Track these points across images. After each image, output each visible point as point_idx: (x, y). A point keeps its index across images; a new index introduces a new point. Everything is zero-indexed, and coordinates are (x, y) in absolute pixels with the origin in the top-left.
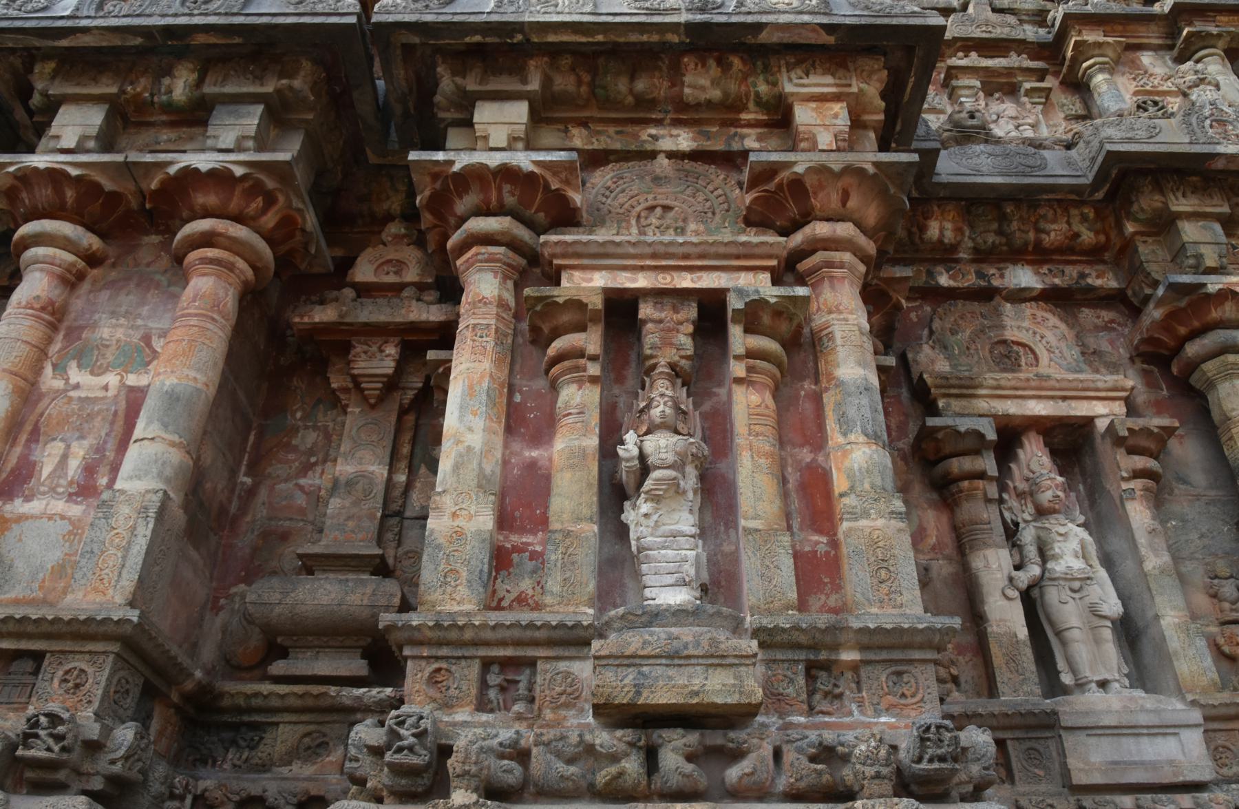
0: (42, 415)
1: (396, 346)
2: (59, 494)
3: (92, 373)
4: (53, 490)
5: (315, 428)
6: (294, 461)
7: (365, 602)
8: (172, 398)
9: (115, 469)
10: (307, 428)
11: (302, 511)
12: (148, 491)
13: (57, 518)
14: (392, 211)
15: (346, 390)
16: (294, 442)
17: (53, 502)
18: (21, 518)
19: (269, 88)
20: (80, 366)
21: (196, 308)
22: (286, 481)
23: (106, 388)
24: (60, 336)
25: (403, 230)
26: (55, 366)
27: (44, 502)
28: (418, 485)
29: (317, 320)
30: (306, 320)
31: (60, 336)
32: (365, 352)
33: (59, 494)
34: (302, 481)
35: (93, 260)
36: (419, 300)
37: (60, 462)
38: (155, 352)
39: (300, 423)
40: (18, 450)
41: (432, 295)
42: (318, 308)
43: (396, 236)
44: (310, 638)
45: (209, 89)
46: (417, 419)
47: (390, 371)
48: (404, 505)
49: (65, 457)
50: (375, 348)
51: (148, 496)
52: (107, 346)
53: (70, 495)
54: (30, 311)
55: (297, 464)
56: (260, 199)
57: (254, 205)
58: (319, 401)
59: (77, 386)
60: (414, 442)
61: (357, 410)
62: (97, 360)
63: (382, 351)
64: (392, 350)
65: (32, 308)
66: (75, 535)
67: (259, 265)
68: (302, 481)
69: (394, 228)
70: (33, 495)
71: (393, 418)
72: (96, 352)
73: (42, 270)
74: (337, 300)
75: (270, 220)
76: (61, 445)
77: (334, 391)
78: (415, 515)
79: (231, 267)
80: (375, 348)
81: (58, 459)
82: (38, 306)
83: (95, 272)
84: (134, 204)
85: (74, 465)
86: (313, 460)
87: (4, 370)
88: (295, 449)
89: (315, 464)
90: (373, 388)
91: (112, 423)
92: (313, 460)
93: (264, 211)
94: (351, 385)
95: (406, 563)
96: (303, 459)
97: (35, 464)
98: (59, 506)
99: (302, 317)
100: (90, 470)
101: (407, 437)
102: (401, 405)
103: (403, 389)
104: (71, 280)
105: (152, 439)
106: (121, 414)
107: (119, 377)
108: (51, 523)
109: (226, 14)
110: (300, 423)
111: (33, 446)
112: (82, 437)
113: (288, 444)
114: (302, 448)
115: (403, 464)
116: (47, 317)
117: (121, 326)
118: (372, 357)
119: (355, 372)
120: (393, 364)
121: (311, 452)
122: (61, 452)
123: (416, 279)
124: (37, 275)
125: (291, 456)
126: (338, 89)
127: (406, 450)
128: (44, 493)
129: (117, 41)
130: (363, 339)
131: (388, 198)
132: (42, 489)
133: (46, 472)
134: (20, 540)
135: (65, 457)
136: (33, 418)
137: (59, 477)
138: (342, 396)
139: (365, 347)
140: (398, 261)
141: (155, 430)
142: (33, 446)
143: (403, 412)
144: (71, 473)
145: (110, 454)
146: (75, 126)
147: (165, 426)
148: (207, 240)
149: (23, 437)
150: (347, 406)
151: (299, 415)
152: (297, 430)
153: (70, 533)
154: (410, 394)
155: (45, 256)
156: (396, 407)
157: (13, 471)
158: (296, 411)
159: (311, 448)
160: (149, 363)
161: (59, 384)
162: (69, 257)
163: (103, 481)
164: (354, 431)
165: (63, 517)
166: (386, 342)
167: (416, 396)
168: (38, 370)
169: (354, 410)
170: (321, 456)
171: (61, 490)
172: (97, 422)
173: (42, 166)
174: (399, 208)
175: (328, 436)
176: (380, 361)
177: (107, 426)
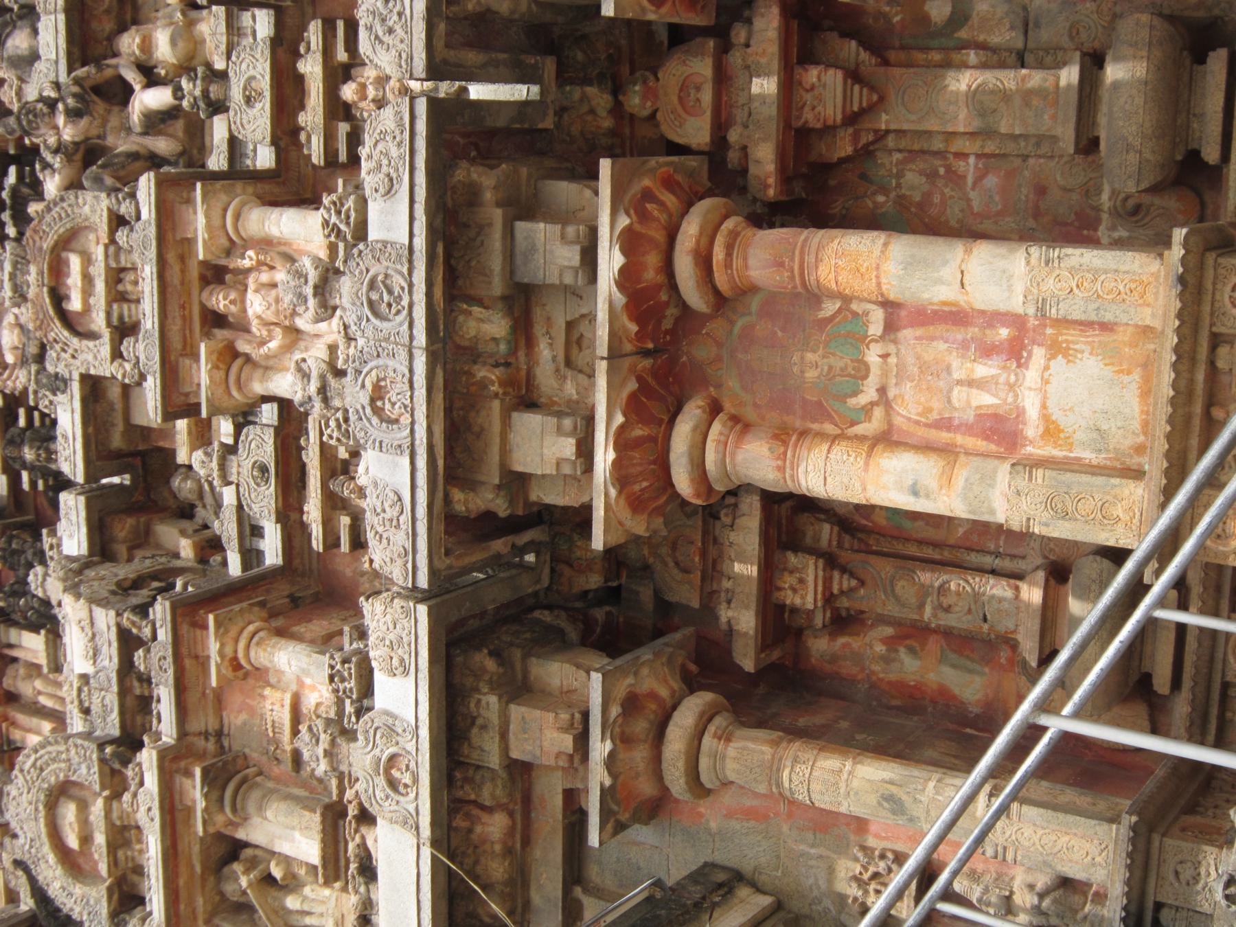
0: (917, 423)
1: (806, 70)
2: (1017, 380)
3: (866, 377)
4: (1011, 387)
5: (900, 175)
6: (943, 194)
7: (1145, 53)
8: (910, 265)
9: (994, 318)
10: (899, 186)
11: (1010, 174)
12: (1028, 263)
13: (1046, 375)
14: (609, 106)
15: (856, 137)
16: (918, 199)
17: (1027, 383)
18: (1046, 417)
19: (497, 215)
20: (855, 393)
21: (792, 260)
22: (969, 200)
23: (885, 356)
24: (815, 426)
25: (637, 88)
26: (853, 423)
27: (1027, 393)
28: (981, 38)
29: (771, 167)
30: (771, 181)
31: (815, 426)
32: (813, 108)
33: (1017, 380)
34: (970, 180)
35: (715, 409)
36: (747, 46)
37: (978, 388)
38: (840, 310)
39: (893, 195)
40: (959, 439)
41: (739, 34)
42: (753, 170)
43: (645, 98)
44: (1179, 121)
45: (497, 287)
46: (893, 48)
47: (840, 75)
48: (1010, 51)
49: (971, 383)
50: (808, 97)
51: (1034, 261)
52: (830, 368)
53: (1019, 366)
54: (789, 454)
55: (946, 191)
56: (648, 206)
57: (656, 213)
58: (863, 176)
59: (882, 390)
60: (926, 49)
61: (884, 117)
62: (850, 375)
63: (813, 88)
64: (812, 74)
65: (785, 453)
66: (1068, 348)
67: (723, 211)
68: (970, 180)
69: (635, 101)
70: (1017, 407)
71: (897, 71)
72: (838, 379)
73: (733, 455)
74: (744, 148)
75: (670, 200)
76: (957, 389)
77: (855, 150)
78: (1021, 37)
79: (734, 235)
80: (808, 97)
81: (974, 391)
82: (782, 449)
83: (727, 406)
84: (647, 363)
85: (982, 370)
86: (942, 171)
87: (867, 464)
88: (927, 196)
89: (949, 169)
90: (860, 97)
91: (933, 339)
92: (942, 171)
93: (662, 204)
94: (850, 130)
95: (1084, 36)
96: (940, 183)
97: (979, 416)
98: (1032, 376)
99: (767, 186)
100: (987, 351)
101: (920, 56)
102: (880, 65)
103: (858, 65)
104: (742, 426)
105: (962, 272)
106: (919, 332)
107: (872, 346)
108: (1053, 380)
109: (410, 261)
110: (893, 195)
111: (956, 422)
112: (948, 369)
113: (920, 206)
114: (926, 188)
115: (956, 57)
116: (794, 438)
117: (802, 358)
118: (820, 99)
119: (839, 117)
120: (831, 72)
121: (932, 175)
122: (965, 389)
123: (709, 61)
124: (740, 457)
125: (937, 199)
126: (473, 154)
127: (937, 57)
128: (1016, 396)
129: (439, 398)
130: (795, 113)
131: (592, 111)
132: (1010, 400)
133: (986, 399)
134: (1071, 409)
135: (971, 383)
136: (922, 432)
137: (997, 383)
138: (863, 141)
139: (807, 109)
140: (681, 90)
141: (949, 272)
142: (956, 422)
143: (886, 63)
144: (993, 371)
145: (973, 331)
146: (540, 447)
147: (945, 263)
148: (704, 261)
149: (945, 436)
150: (876, 131)
151: (881, 199)
152: (903, 197)
153: (1065, 356)
154: (864, 55)
155: (717, 451)
156: (882, 69)
157: (987, 438)
158: (874, 202)
159: (927, 176)
160: (855, 314)
161: (878, 413)
162: (716, 427)
163: (1004, 333)
164: (914, 117)
165: (1047, 368)
166: (800, 84)
167: (866, 49)
168: (861, 439)
169: (884, 121)
170: (938, 162)
171: (1013, 378)
172: (928, 356)
173: (611, 455)
174: (605, 96)
175: (913, 155)
176: (827, 91)
177: (935, 343)
